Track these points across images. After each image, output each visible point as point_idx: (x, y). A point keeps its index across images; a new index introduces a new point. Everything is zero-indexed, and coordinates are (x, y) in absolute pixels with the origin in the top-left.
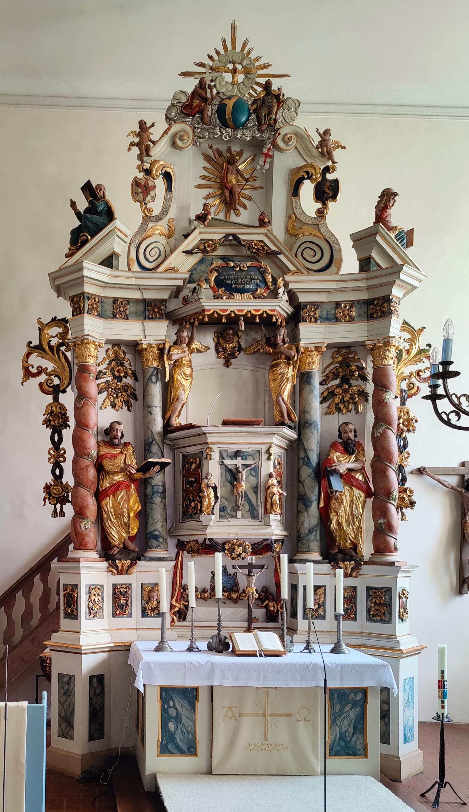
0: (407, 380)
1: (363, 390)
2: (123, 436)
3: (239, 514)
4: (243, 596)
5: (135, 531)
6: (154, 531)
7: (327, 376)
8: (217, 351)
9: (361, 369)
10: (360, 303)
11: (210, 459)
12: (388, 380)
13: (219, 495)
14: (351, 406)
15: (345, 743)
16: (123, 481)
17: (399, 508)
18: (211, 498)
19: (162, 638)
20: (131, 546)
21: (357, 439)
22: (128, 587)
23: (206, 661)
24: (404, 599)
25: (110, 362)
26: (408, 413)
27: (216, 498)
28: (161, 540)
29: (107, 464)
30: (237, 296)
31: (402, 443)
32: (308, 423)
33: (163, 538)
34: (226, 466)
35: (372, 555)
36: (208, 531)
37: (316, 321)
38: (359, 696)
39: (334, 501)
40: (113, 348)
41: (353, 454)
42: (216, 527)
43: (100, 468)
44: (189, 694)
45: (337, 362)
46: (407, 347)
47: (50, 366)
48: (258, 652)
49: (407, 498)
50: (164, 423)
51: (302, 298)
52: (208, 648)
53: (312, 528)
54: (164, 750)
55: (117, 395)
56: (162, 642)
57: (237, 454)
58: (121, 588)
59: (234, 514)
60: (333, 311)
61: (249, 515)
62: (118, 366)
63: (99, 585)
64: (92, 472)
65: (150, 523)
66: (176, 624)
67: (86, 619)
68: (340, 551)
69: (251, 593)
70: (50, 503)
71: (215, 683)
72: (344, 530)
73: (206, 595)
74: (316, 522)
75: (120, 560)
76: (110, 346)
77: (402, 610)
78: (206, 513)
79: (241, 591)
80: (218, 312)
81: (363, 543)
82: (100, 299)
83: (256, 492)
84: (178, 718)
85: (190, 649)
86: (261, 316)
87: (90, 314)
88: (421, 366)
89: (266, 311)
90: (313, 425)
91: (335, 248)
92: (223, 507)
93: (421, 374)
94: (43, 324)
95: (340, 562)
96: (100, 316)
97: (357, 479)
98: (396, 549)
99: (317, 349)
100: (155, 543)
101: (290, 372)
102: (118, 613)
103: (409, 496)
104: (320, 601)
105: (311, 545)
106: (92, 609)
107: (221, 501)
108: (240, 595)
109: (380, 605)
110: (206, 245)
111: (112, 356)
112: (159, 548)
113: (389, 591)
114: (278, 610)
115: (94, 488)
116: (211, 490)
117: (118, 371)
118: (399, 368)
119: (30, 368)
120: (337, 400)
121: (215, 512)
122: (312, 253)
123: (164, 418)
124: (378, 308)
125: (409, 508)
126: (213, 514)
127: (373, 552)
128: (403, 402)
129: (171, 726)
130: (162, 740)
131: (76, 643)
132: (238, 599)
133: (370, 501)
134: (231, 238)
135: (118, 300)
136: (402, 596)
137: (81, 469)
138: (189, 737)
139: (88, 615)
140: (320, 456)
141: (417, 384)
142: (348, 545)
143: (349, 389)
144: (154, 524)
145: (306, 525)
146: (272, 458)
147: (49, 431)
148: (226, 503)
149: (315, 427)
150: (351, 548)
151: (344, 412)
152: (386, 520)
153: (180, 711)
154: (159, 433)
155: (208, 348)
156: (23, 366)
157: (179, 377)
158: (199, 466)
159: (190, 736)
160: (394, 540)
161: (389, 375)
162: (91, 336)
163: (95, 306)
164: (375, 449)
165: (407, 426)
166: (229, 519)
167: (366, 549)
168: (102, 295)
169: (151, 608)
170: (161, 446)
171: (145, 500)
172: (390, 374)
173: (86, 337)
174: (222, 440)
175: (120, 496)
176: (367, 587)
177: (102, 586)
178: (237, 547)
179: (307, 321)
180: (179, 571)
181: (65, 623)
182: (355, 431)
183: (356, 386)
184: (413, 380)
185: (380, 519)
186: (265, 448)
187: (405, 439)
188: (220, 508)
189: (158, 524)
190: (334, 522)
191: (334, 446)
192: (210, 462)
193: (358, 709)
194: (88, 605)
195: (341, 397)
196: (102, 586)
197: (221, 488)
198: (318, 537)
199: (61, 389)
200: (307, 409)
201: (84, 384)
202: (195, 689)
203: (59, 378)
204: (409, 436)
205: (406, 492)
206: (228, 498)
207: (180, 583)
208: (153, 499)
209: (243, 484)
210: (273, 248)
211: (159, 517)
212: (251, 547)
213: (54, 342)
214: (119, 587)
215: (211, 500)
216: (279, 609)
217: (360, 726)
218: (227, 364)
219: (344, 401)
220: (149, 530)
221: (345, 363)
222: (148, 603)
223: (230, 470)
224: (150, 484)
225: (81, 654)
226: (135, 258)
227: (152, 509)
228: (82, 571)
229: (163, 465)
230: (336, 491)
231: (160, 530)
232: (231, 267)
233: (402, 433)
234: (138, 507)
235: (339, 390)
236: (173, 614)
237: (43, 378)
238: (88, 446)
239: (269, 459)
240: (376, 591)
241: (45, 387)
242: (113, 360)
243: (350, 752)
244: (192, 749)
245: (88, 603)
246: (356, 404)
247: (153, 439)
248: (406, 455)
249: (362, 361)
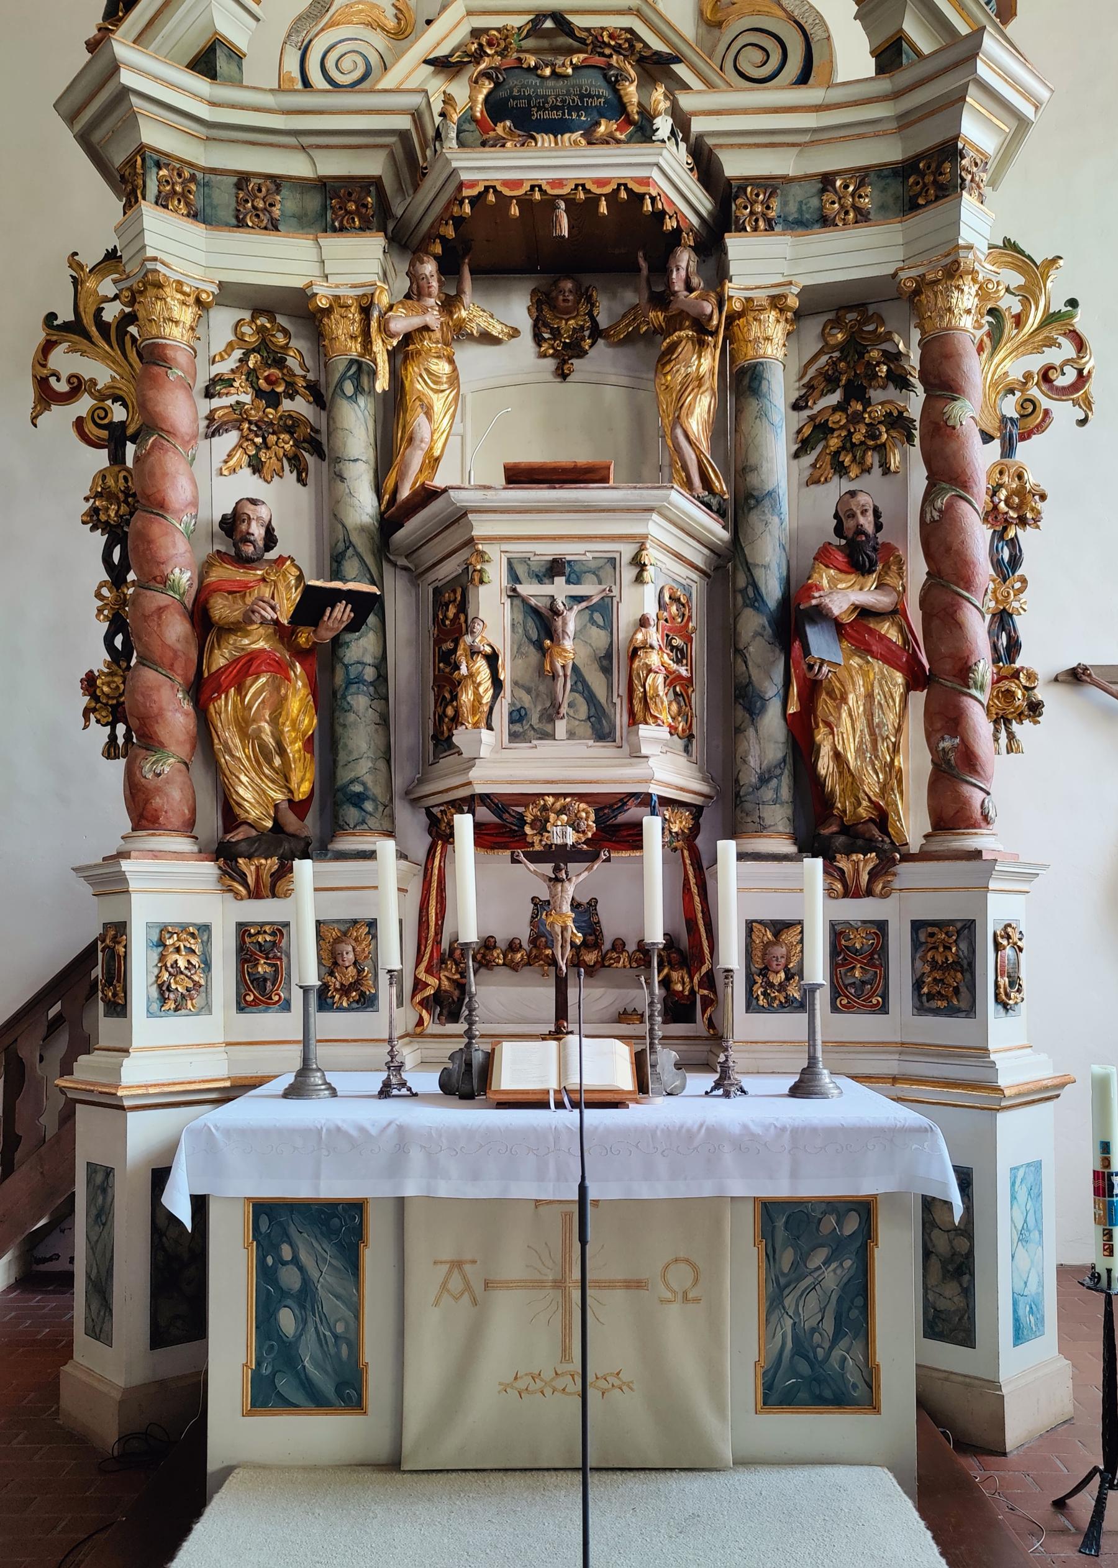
0: (1018, 394)
1: (901, 413)
2: (270, 540)
3: (561, 727)
4: (611, 958)
5: (303, 790)
6: (352, 782)
7: (810, 387)
8: (538, 339)
9: (894, 357)
10: (885, 173)
11: (482, 582)
12: (959, 367)
13: (505, 675)
14: (872, 458)
15: (812, 1365)
16: (263, 650)
17: (1001, 721)
18: (479, 684)
19: (306, 1060)
20: (291, 821)
21: (881, 537)
22: (280, 930)
23: (385, 1123)
24: (1009, 951)
25: (247, 355)
26: (1020, 477)
27: (497, 684)
28: (368, 806)
29: (222, 609)
30: (545, 140)
31: (1006, 555)
32: (752, 496)
33: (374, 800)
34: (524, 600)
35: (926, 836)
36: (473, 774)
37: (770, 227)
38: (852, 1225)
39: (824, 696)
40: (253, 319)
41: (870, 572)
42: (495, 760)
43: (200, 617)
44: (339, 1224)
45: (833, 348)
46: (1017, 308)
47: (101, 373)
48: (552, 1093)
49: (1019, 694)
50: (380, 505)
51: (735, 165)
52: (442, 1086)
53: (769, 771)
54: (265, 1396)
55: (264, 439)
56: (304, 1071)
57: (555, 568)
58: (259, 933)
59: (548, 728)
60: (815, 202)
61: (590, 731)
62: (269, 366)
63: (194, 925)
64: (176, 630)
65: (341, 763)
66: (429, 1031)
67: (150, 1014)
68: (845, 830)
69: (558, 929)
70: (98, 721)
71: (410, 1190)
72: (852, 774)
73: (519, 955)
74: (780, 755)
75: (250, 857)
76: (247, 315)
77: (1004, 981)
78: (470, 726)
79: (607, 946)
80: (499, 188)
81: (907, 810)
82: (199, 175)
83: (607, 670)
84: (306, 1298)
85: (385, 1092)
86: (612, 198)
87: (166, 207)
88: (1051, 357)
89: (625, 185)
90: (767, 502)
91: (816, 34)
92: (519, 711)
93: (1053, 375)
94: (81, 267)
95: (838, 856)
96: (194, 215)
97: (883, 638)
98: (986, 818)
99: (777, 302)
100: (351, 814)
101: (707, 363)
102: (250, 998)
103: (1026, 688)
104: (788, 961)
105: (764, 815)
106: (169, 989)
107: (513, 696)
108: (604, 958)
109: (946, 967)
110: (484, 40)
111: (252, 339)
112: (365, 827)
113: (967, 929)
114: (693, 992)
115: (183, 671)
116: (481, 665)
117: (267, 379)
118: (996, 360)
119: (52, 380)
120: (834, 442)
121: (495, 723)
122: (759, 56)
123: (378, 491)
124: (928, 177)
125: (1026, 722)
126: (490, 728)
127: (929, 829)
128: (1008, 450)
129: (287, 1320)
130: (258, 1364)
131: (104, 1081)
132: (598, 966)
133: (919, 698)
134: (549, 24)
135: (248, 180)
136: (1005, 942)
137: (146, 618)
138: (338, 1354)
139: (155, 1006)
140: (787, 582)
141: (1045, 403)
142: (863, 812)
143: (865, 410)
144: (350, 766)
145: (753, 762)
146: (649, 573)
147: (99, 539)
148: (526, 700)
149: (773, 507)
150: (871, 820)
151: (852, 475)
152: (958, 740)
153: (314, 1273)
154: (363, 529)
155: (515, 333)
156: (34, 376)
157: (418, 385)
158: (463, 607)
159: (344, 1349)
160: (982, 795)
161: (960, 355)
162: (163, 263)
163: (178, 188)
164: (929, 556)
165: (1018, 508)
166: (535, 742)
167: (913, 823)
168: (202, 163)
169: (342, 984)
170: (369, 560)
171: (328, 703)
172: (962, 352)
173: (150, 265)
174: (511, 533)
175: (252, 690)
176: (913, 922)
177: (206, 928)
178: (552, 816)
179: (748, 229)
180: (434, 893)
181: (106, 1027)
182: (877, 514)
183: (882, 404)
184: (1034, 392)
185: (943, 739)
186: (627, 551)
187: (1013, 543)
188: (510, 714)
189: (361, 764)
190: (825, 751)
191: (823, 556)
192: (482, 589)
193: (848, 1263)
194: (158, 977)
195: (844, 433)
196: (206, 928)
197: (513, 658)
198: (785, 793)
199: (130, 431)
200: (752, 461)
201: (151, 393)
202: (356, 1208)
203: (125, 405)
204: (1026, 537)
205: (1018, 678)
206: (533, 685)
207: (436, 924)
208: (349, 698)
209: (568, 644)
210: (657, 45)
211: (364, 746)
212: (592, 816)
213: (111, 312)
214: (252, 931)
215: (481, 690)
216: (696, 989)
217: (854, 1313)
218: (562, 374)
219: (853, 445)
220: (340, 783)
221: (854, 348)
222: (332, 974)
223: (535, 612)
224: (341, 660)
225: (122, 1108)
226: (296, 74)
227: (345, 726)
228: (132, 886)
229: (366, 607)
230: (822, 662)
231: (368, 779)
232: (529, 69)
233: (1005, 529)
234: (311, 721)
235: (839, 418)
236: (421, 1003)
237: (84, 405)
238: (162, 554)
239: (639, 579)
240: (935, 930)
241: (90, 428)
242: (254, 350)
243: (828, 1394)
244: (347, 1393)
245: (156, 971)
246: (881, 449)
247: (349, 544)
248: (1018, 585)
249: (896, 338)
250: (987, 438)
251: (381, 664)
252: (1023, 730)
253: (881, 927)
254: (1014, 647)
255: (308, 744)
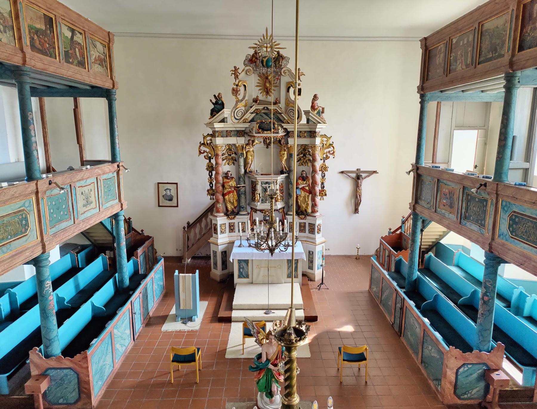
20: (234, 210)
43: (223, 186)
44: (247, 262)
47: (208, 150)
54: (239, 277)
57: (267, 183)
84: (243, 268)
115: (222, 193)
129: (241, 270)
147: (208, 172)
186: (275, 181)
189: (243, 203)
204: (326, 173)
213: (209, 142)
237: (205, 154)
244: (247, 276)
250: (321, 160)
251: (245, 191)
252: (324, 197)
253: (305, 223)
254: (324, 187)
255: (236, 201)
